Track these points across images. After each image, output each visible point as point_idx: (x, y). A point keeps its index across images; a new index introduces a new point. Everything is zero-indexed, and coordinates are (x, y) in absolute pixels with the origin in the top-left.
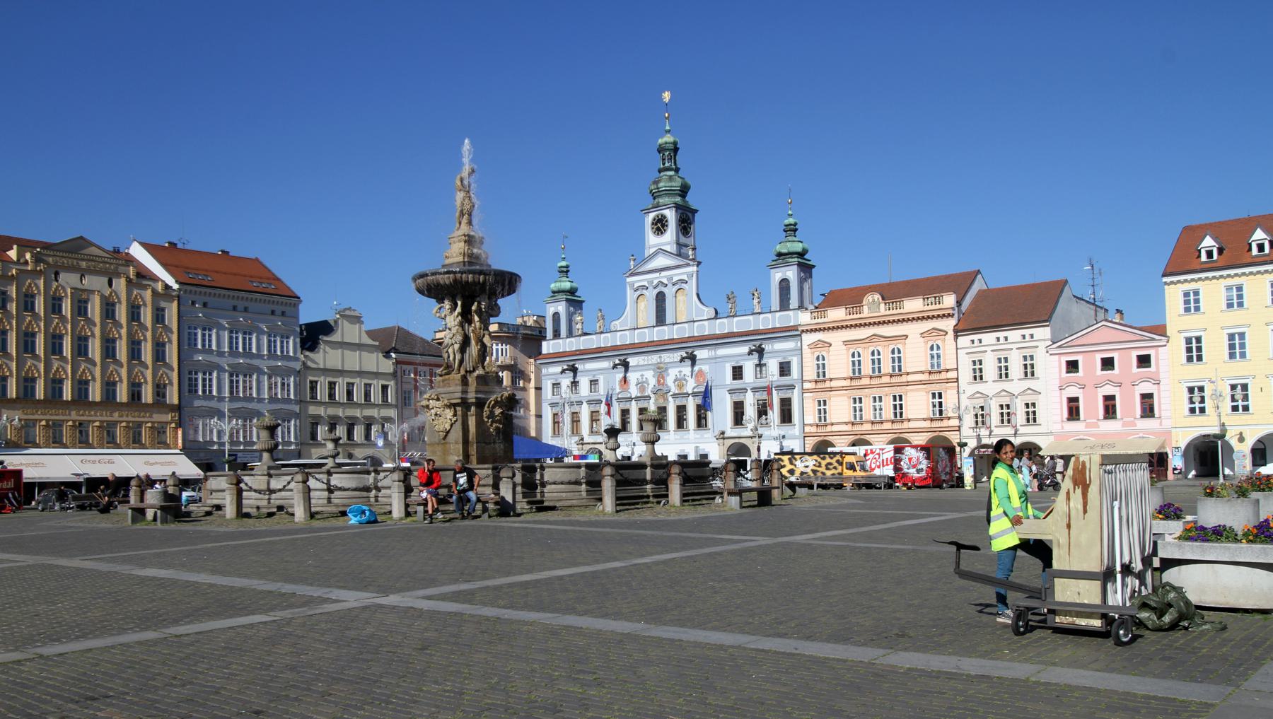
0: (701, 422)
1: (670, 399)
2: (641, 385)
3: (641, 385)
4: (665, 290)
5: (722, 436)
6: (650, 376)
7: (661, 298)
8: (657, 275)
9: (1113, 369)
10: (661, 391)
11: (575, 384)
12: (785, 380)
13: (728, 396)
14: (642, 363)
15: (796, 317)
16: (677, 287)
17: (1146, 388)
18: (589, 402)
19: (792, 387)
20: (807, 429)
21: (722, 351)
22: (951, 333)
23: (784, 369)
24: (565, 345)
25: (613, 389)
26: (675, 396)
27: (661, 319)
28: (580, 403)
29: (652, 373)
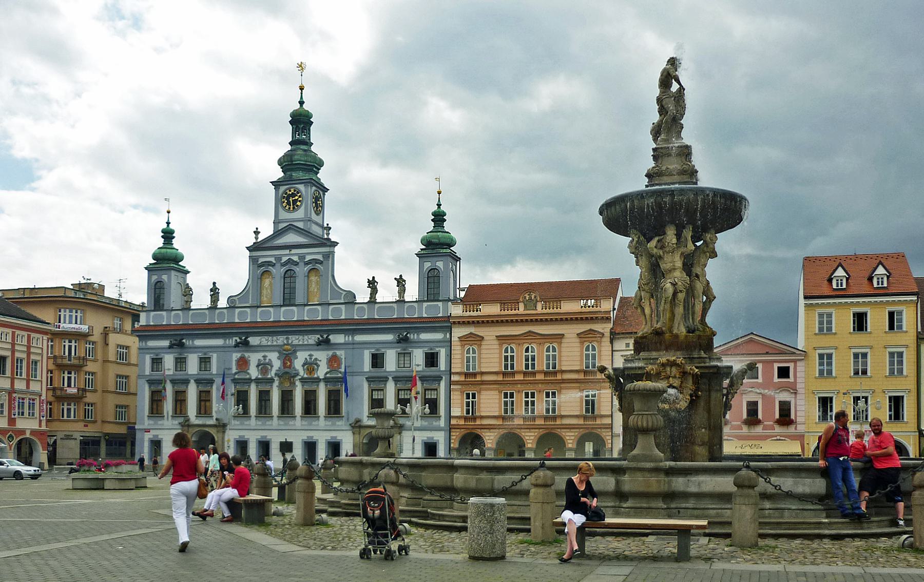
0: (334, 409)
1: (298, 383)
2: (264, 366)
3: (264, 366)
4: (297, 269)
5: (357, 426)
6: (273, 357)
7: (289, 276)
8: (287, 252)
9: (779, 377)
10: (287, 375)
11: (180, 362)
12: (432, 371)
13: (366, 385)
14: (264, 342)
15: (446, 309)
17: (785, 396)
18: (198, 382)
19: (438, 379)
20: (453, 422)
21: (359, 338)
22: (607, 334)
23: (431, 359)
24: (169, 318)
25: (230, 369)
26: (303, 380)
27: (288, 300)
28: (186, 382)
29: (277, 354)
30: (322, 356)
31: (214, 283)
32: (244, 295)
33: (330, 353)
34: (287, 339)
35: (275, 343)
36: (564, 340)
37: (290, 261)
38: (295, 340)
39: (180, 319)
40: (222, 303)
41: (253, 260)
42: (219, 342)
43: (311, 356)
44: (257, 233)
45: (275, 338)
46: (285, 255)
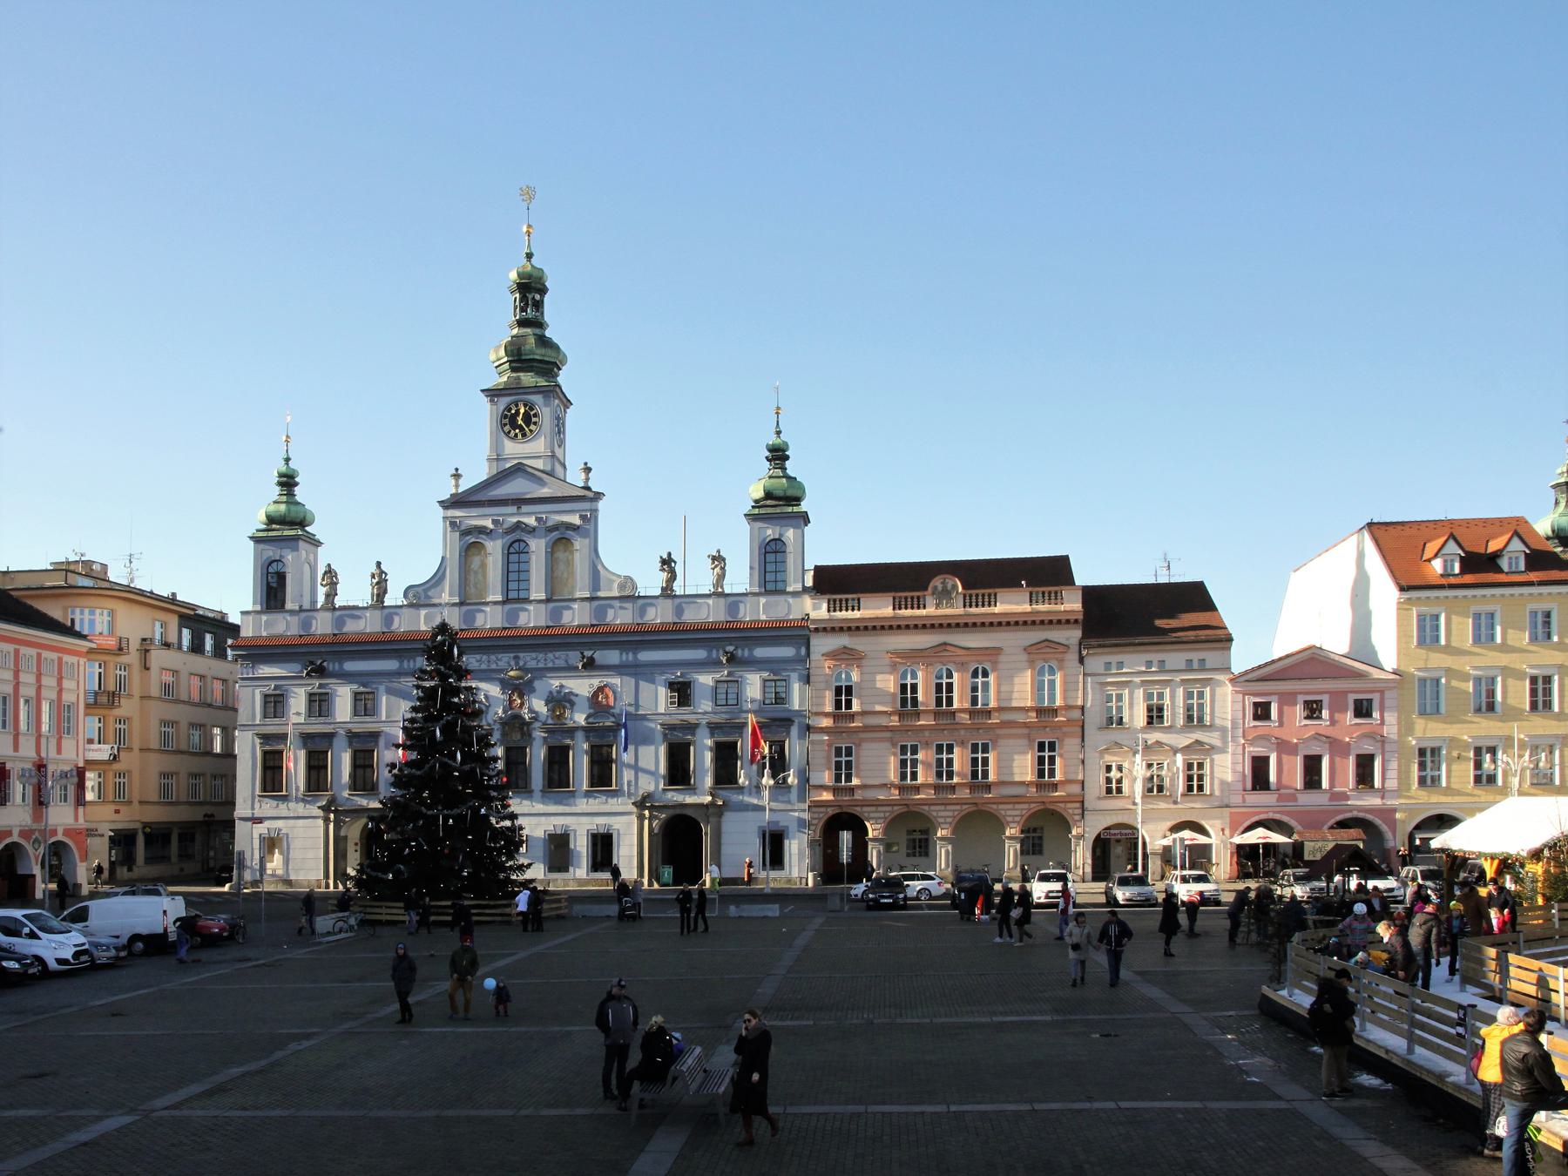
1: (538, 734)
8: (513, 509)
16: (555, 535)
21: (646, 656)
30: (582, 686)
31: (379, 564)
33: (596, 682)
34: (516, 658)
35: (494, 666)
36: (1002, 658)
37: (518, 525)
38: (530, 659)
39: (322, 626)
40: (394, 597)
44: (457, 476)
45: (493, 657)
46: (511, 517)
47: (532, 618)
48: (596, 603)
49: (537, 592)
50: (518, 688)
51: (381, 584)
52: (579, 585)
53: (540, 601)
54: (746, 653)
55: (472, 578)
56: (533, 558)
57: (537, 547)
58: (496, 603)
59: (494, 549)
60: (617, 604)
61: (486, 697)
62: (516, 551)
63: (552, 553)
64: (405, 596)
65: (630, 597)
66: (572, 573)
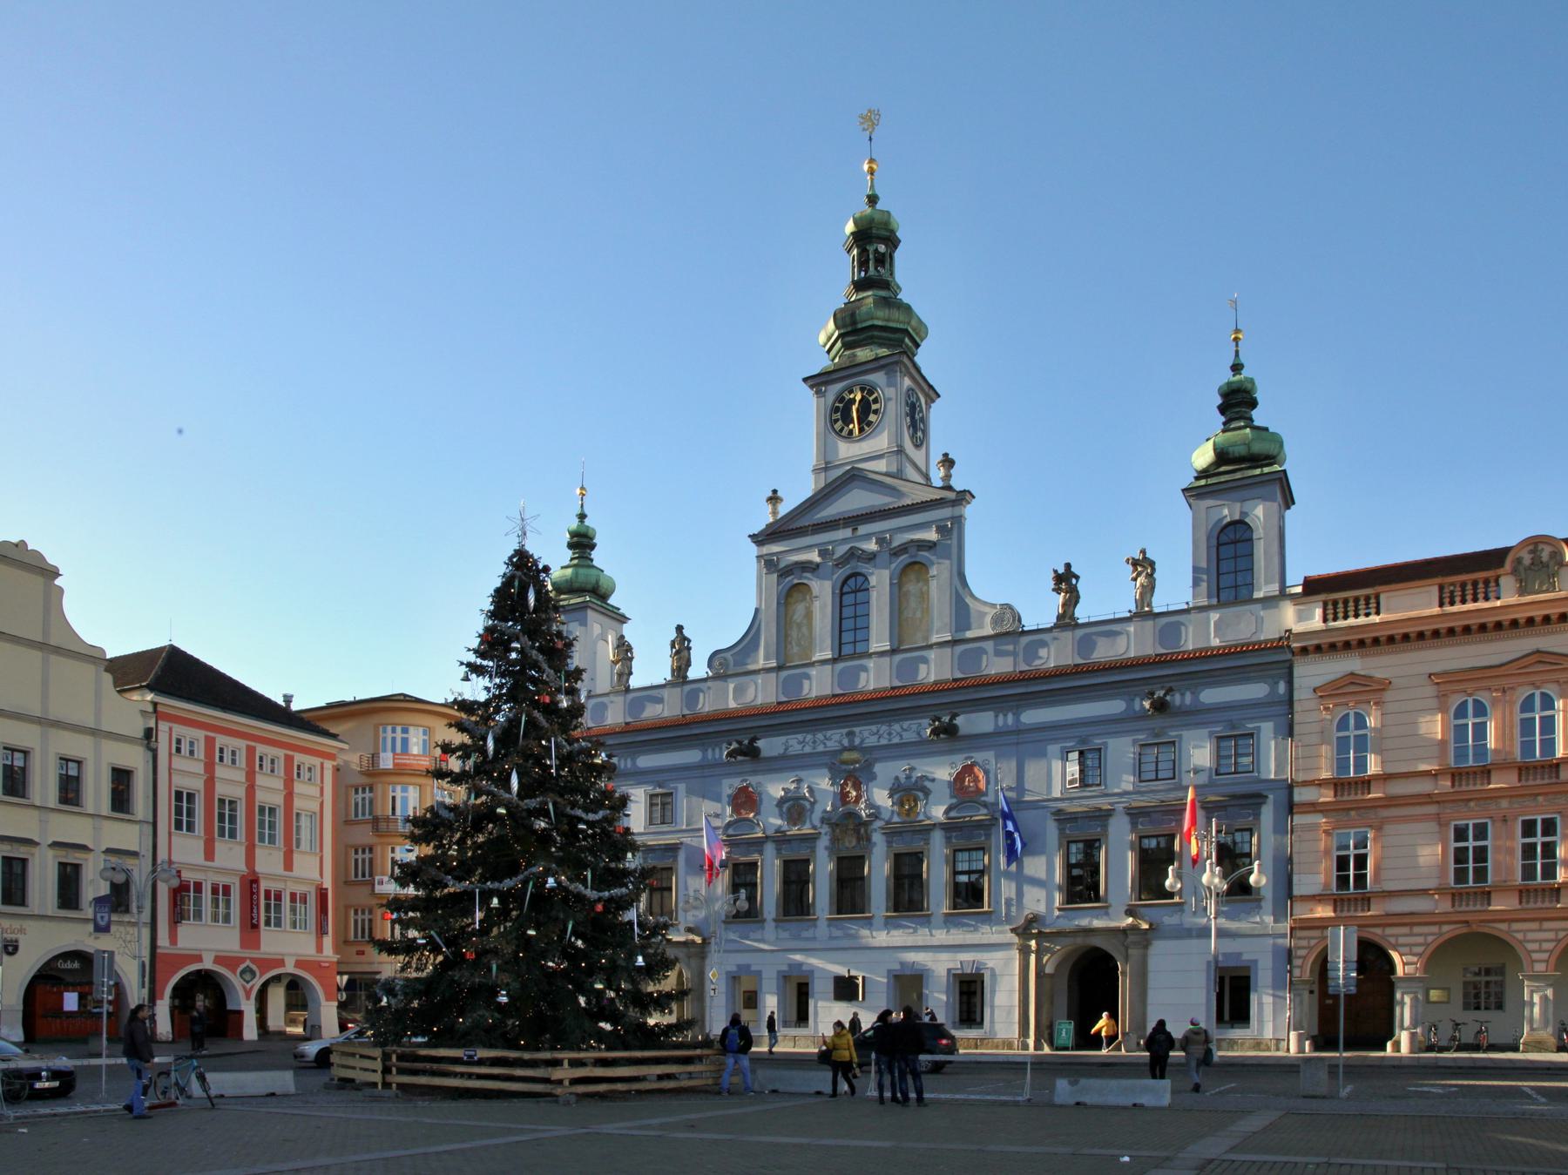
4: (864, 568)
21: (1032, 717)
30: (942, 771)
32: (749, 641)
33: (960, 761)
34: (851, 734)
35: (821, 748)
38: (868, 735)
41: (769, 563)
42: (692, 756)
43: (912, 769)
44: (774, 498)
45: (820, 736)
47: (875, 677)
48: (960, 648)
49: (879, 641)
50: (853, 774)
51: (681, 647)
52: (937, 624)
53: (882, 654)
54: (1188, 698)
55: (794, 633)
56: (874, 595)
57: (880, 580)
58: (824, 662)
59: (822, 590)
60: (989, 646)
61: (811, 790)
62: (852, 590)
63: (900, 585)
64: (710, 666)
65: (1011, 632)
66: (927, 610)
